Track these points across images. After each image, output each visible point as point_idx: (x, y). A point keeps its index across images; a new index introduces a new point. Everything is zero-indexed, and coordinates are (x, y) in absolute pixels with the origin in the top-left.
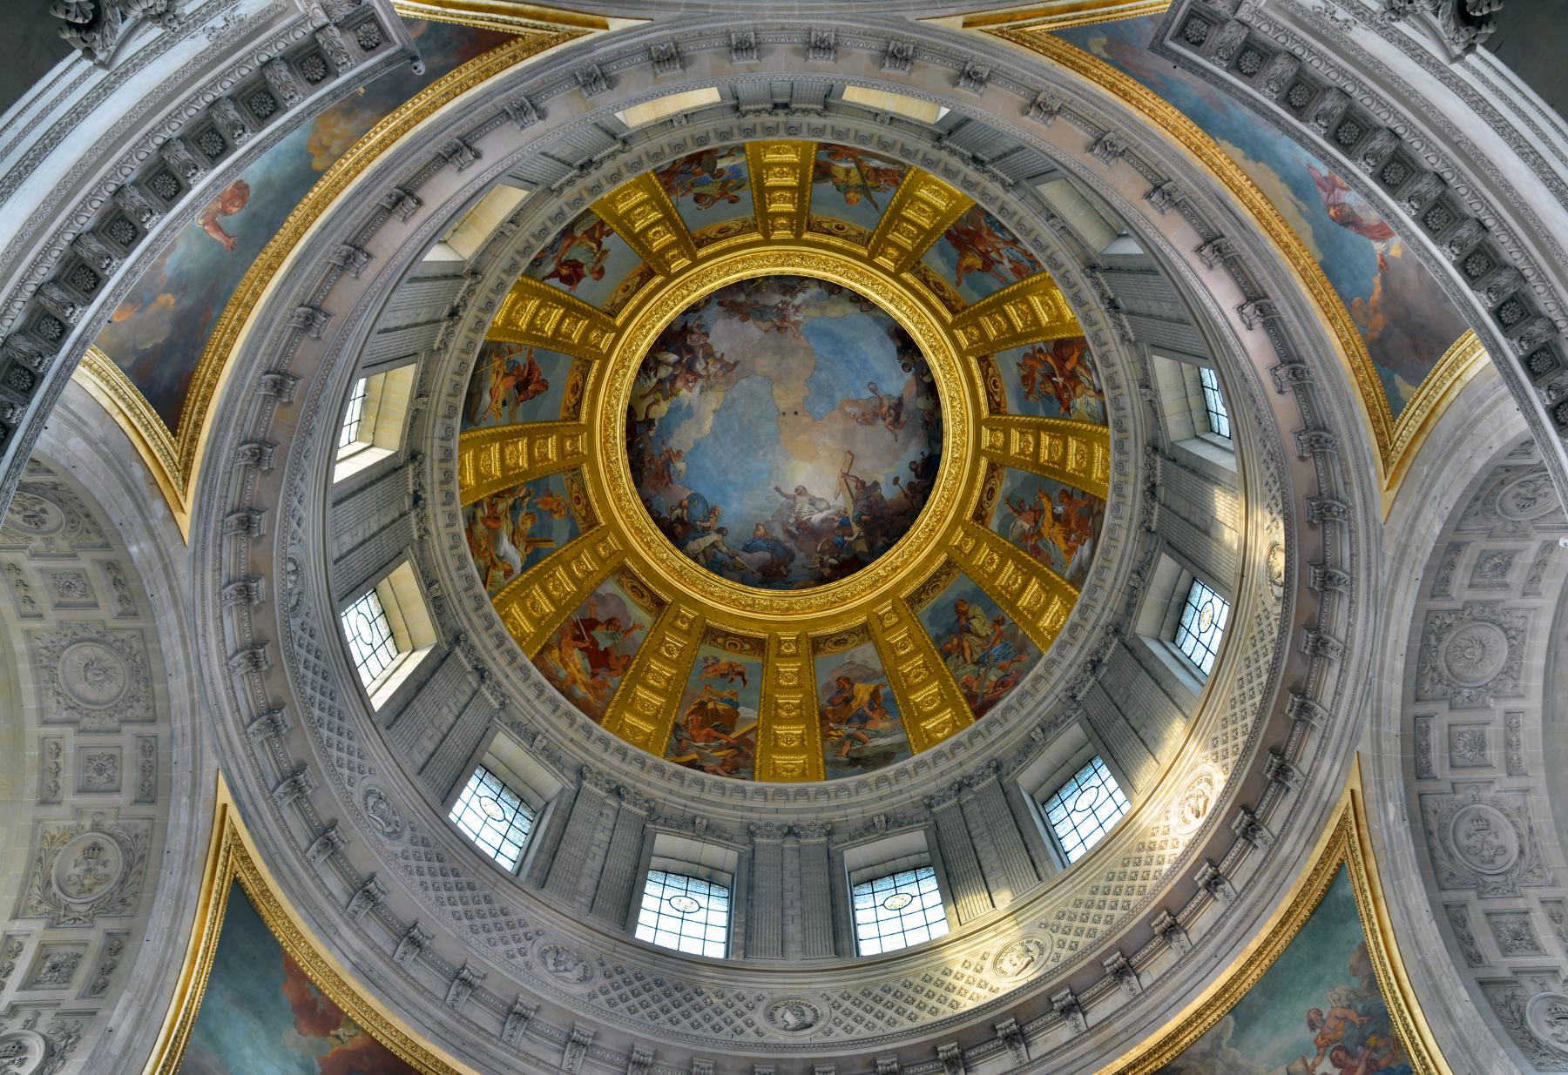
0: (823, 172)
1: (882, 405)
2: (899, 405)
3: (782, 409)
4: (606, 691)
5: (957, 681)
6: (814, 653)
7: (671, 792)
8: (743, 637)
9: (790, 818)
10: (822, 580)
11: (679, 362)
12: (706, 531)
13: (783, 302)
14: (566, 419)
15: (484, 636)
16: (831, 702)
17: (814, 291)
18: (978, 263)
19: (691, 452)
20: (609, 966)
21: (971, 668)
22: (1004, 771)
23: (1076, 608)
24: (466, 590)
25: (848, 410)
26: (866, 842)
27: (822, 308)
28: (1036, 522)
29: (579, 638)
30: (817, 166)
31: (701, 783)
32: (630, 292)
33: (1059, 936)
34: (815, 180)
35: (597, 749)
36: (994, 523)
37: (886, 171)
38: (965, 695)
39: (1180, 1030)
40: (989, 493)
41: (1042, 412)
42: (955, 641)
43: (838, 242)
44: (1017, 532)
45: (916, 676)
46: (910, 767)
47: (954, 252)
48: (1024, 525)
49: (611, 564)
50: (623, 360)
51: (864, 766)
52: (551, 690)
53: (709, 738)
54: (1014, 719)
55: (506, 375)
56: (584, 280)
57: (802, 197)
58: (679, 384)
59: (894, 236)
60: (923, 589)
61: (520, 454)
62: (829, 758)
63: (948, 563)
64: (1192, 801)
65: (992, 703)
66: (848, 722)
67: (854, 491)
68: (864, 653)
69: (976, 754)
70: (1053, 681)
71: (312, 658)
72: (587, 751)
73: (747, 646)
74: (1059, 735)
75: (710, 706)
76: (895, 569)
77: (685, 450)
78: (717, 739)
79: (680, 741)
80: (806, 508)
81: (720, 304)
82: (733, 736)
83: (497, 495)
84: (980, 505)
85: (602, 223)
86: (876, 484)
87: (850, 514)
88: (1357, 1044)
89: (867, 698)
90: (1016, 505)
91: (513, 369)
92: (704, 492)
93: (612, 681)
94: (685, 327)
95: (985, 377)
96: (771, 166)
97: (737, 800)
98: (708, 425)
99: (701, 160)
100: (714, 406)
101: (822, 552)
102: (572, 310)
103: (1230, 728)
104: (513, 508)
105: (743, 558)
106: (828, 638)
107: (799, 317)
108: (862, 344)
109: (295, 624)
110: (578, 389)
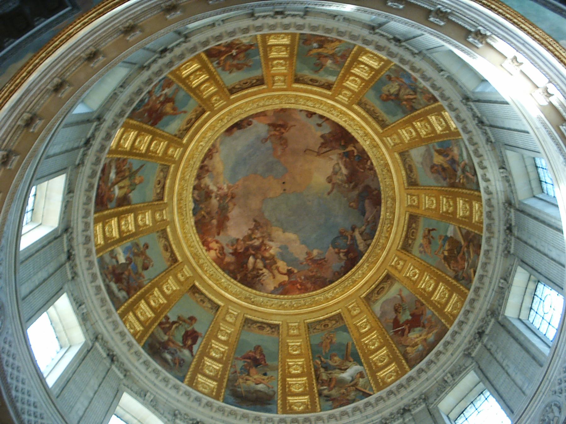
0: (124, 200)
1: (274, 135)
2: (273, 126)
3: (282, 191)
4: (433, 320)
5: (427, 105)
6: (417, 185)
7: (486, 296)
8: (409, 227)
9: (503, 228)
11: (254, 255)
12: (353, 239)
13: (216, 197)
14: (279, 333)
15: (389, 402)
16: (445, 179)
17: (207, 181)
20: (557, 388)
21: (418, 96)
23: (365, 46)
24: (361, 412)
25: (279, 153)
28: (326, 57)
29: (403, 335)
30: (119, 205)
34: (129, 203)
35: (459, 338)
36: (332, 79)
37: (117, 168)
40: (313, 82)
41: (258, 58)
42: (405, 103)
43: (168, 182)
44: (334, 66)
45: (427, 128)
47: (165, 119)
48: (329, 63)
49: (363, 307)
50: (246, 298)
53: (463, 259)
55: (249, 375)
57: (140, 209)
58: (267, 255)
60: (376, 119)
61: (296, 365)
63: (359, 104)
66: (455, 171)
67: (327, 149)
68: (417, 154)
72: (459, 346)
73: (414, 225)
75: (446, 253)
76: (367, 134)
77: (306, 250)
78: (464, 254)
79: (463, 278)
81: (218, 234)
82: (463, 243)
83: (318, 377)
84: (322, 86)
85: (160, 324)
86: (322, 136)
87: (342, 151)
90: (318, 67)
93: (428, 314)
94: (232, 254)
95: (242, 89)
96: (120, 232)
97: (492, 255)
98: (292, 236)
100: (280, 232)
101: (364, 168)
104: (326, 369)
105: (369, 216)
106: (408, 177)
107: (225, 187)
108: (239, 148)
110: (262, 326)
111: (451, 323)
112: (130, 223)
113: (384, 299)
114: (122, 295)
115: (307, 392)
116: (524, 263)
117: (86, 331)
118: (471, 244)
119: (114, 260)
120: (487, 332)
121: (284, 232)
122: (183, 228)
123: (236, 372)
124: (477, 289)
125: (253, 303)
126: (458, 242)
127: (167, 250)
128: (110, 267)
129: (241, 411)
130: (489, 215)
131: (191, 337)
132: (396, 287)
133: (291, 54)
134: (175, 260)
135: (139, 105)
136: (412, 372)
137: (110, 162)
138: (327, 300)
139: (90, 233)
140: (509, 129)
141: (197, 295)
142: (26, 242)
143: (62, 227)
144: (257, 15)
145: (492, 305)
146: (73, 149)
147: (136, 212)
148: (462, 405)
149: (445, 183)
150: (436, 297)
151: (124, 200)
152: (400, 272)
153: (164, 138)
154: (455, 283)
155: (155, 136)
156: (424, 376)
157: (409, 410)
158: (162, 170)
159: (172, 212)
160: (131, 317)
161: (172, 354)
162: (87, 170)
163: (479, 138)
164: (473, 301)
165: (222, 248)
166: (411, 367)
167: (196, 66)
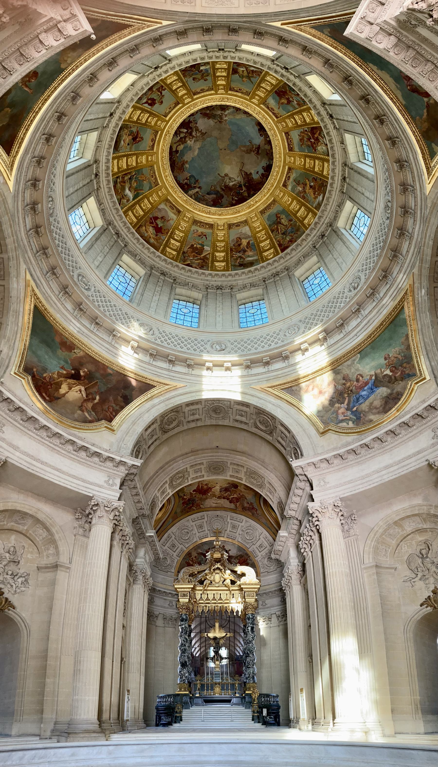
8: (206, 224)
9: (219, 284)
10: (233, 205)
16: (234, 245)
21: (280, 235)
22: (290, 270)
26: (243, 292)
31: (190, 271)
33: (305, 325)
35: (157, 260)
38: (278, 244)
46: (259, 268)
51: (244, 267)
53: (194, 256)
54: (294, 253)
62: (233, 264)
64: (353, 284)
65: (287, 247)
68: (246, 230)
69: (281, 264)
70: (308, 241)
71: (58, 231)
72: (154, 260)
74: (309, 259)
75: (195, 246)
79: (184, 257)
82: (202, 256)
88: (400, 366)
89: (246, 244)
97: (203, 277)
101: (233, 195)
103: (368, 261)
106: (233, 224)
109: (51, 219)
149: (232, 245)
156: (135, 242)
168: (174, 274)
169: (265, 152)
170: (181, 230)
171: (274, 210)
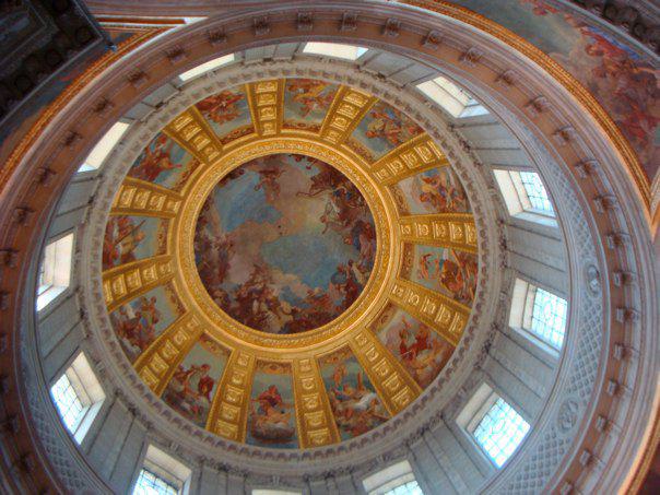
0: (128, 257)
8: (405, 256)
11: (258, 299)
12: (352, 273)
16: (435, 206)
17: (206, 232)
18: (164, 160)
19: (309, 285)
21: (402, 129)
27: (215, 224)
30: (125, 262)
32: (216, 346)
36: (319, 121)
39: (565, 84)
40: (301, 126)
43: (170, 235)
47: (162, 173)
52: (435, 383)
53: (460, 278)
56: (210, 376)
58: (270, 297)
59: (159, 206)
61: (311, 401)
63: (346, 143)
75: (444, 276)
76: (356, 172)
80: (332, 216)
81: (222, 282)
83: (334, 409)
84: (310, 129)
85: (175, 375)
90: (305, 111)
91: (264, 410)
92: (331, 274)
96: (128, 288)
97: (489, 271)
98: (291, 277)
99: (128, 330)
102: (228, 381)
104: (341, 400)
106: (400, 207)
107: (223, 235)
110: (274, 366)
111: (457, 342)
112: (136, 280)
113: (389, 326)
114: (135, 349)
115: (327, 424)
116: (522, 275)
117: (105, 388)
118: (467, 266)
119: (124, 316)
120: (494, 344)
121: (284, 273)
122: (188, 279)
123: (253, 413)
124: (478, 306)
125: (262, 345)
126: (455, 265)
127: (174, 302)
128: (122, 326)
129: (264, 450)
130: (483, 233)
131: (207, 384)
132: (399, 313)
133: (279, 100)
134: (182, 311)
135: (137, 162)
136: (426, 392)
137: (113, 219)
138: (334, 334)
139: (100, 290)
140: (497, 149)
141: (208, 343)
142: (43, 302)
143: (73, 286)
144: (247, 63)
145: (496, 318)
146: (79, 208)
147: (141, 267)
148: (478, 417)
149: (435, 210)
150: (439, 319)
151: (128, 257)
152: (401, 298)
153: (161, 192)
154: (455, 303)
155: (154, 191)
156: (437, 395)
157: (428, 429)
158: (163, 224)
159: (175, 264)
160: (146, 370)
161: (190, 403)
162: (91, 228)
163: (467, 162)
164: (475, 318)
165: (226, 296)
166: (424, 388)
167: (188, 119)
168: (488, 328)
169: (271, 167)
170: (420, 302)
171: (363, 142)
